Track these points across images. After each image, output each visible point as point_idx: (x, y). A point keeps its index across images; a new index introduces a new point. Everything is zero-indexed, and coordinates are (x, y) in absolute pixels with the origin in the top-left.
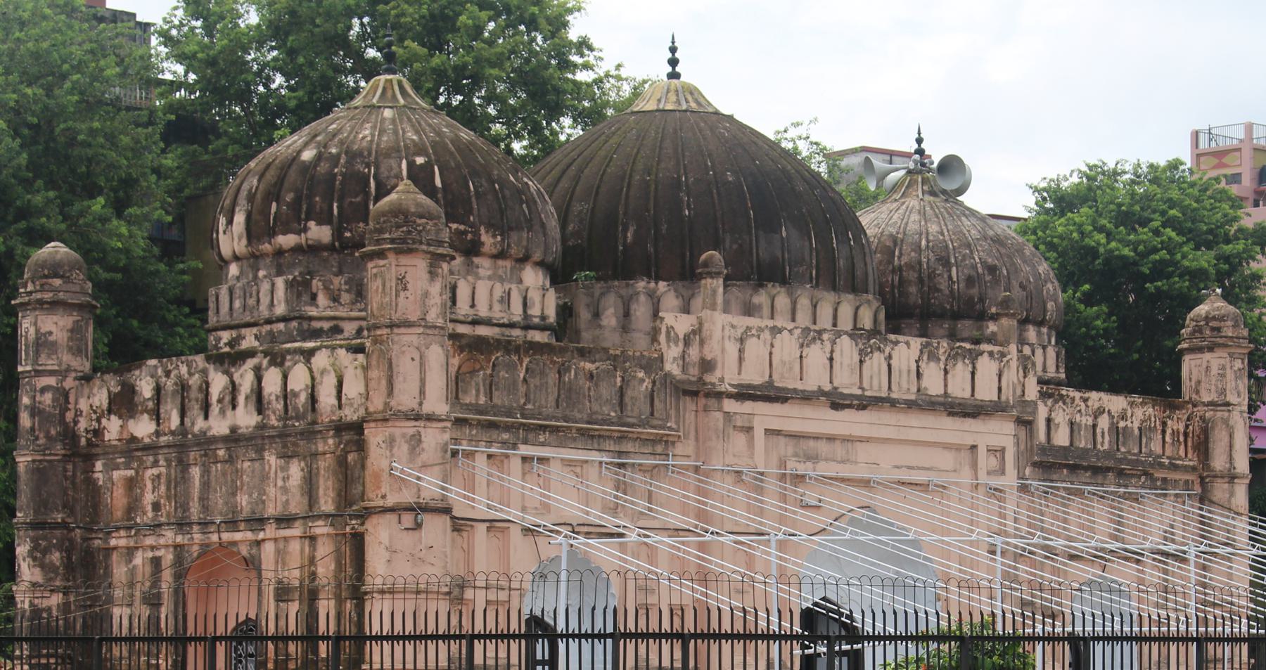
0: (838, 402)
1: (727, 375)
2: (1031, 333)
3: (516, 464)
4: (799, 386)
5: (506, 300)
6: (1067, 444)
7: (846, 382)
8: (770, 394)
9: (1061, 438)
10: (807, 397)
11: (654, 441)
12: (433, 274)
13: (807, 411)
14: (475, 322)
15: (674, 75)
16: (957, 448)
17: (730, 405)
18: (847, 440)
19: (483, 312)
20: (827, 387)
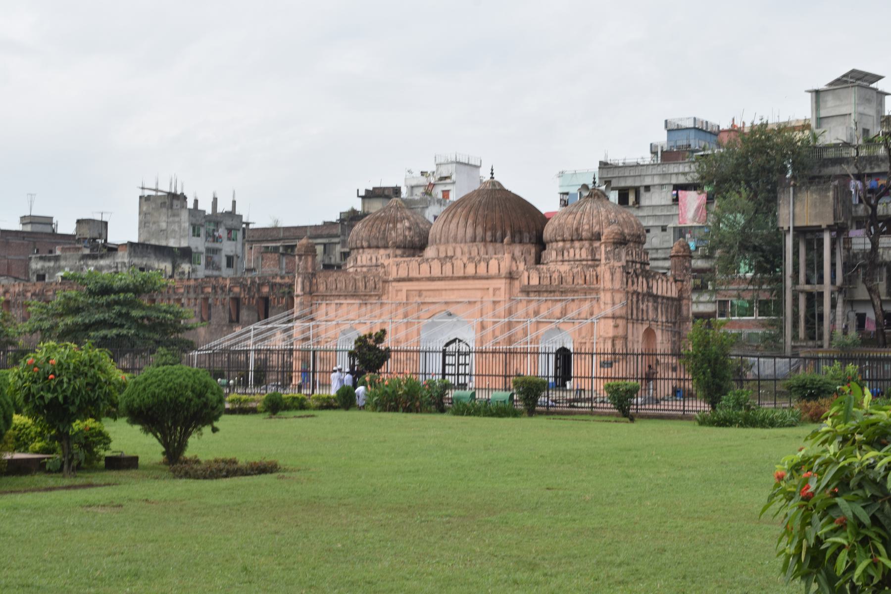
0: (431, 279)
1: (393, 275)
2: (577, 244)
3: (333, 306)
4: (418, 276)
5: (371, 259)
6: (537, 283)
7: (436, 272)
8: (409, 279)
9: (535, 281)
10: (418, 280)
11: (376, 295)
12: (300, 259)
13: (422, 283)
14: (362, 267)
15: (492, 178)
16: (483, 289)
17: (394, 284)
18: (438, 290)
19: (364, 263)
20: (428, 275)
